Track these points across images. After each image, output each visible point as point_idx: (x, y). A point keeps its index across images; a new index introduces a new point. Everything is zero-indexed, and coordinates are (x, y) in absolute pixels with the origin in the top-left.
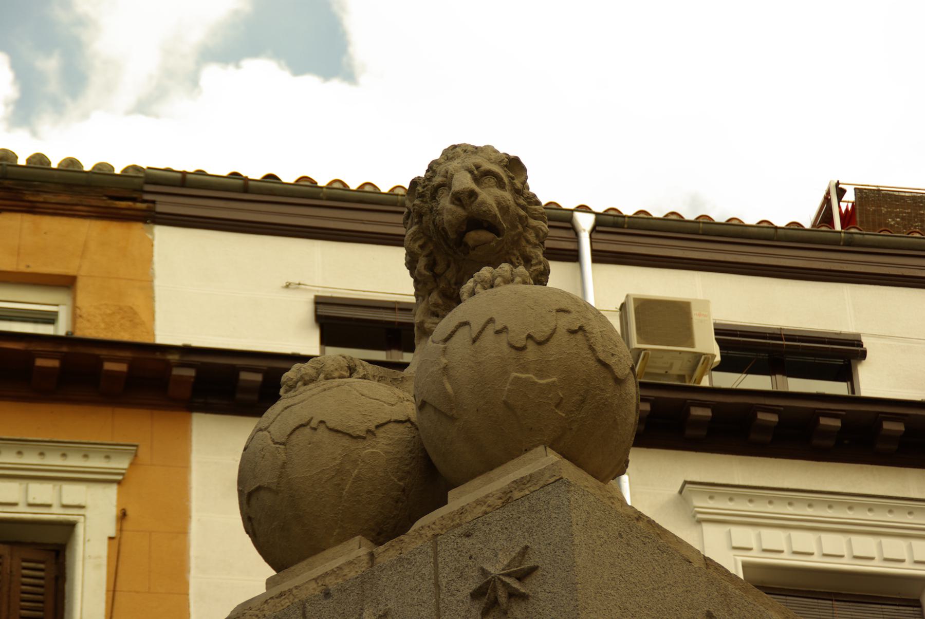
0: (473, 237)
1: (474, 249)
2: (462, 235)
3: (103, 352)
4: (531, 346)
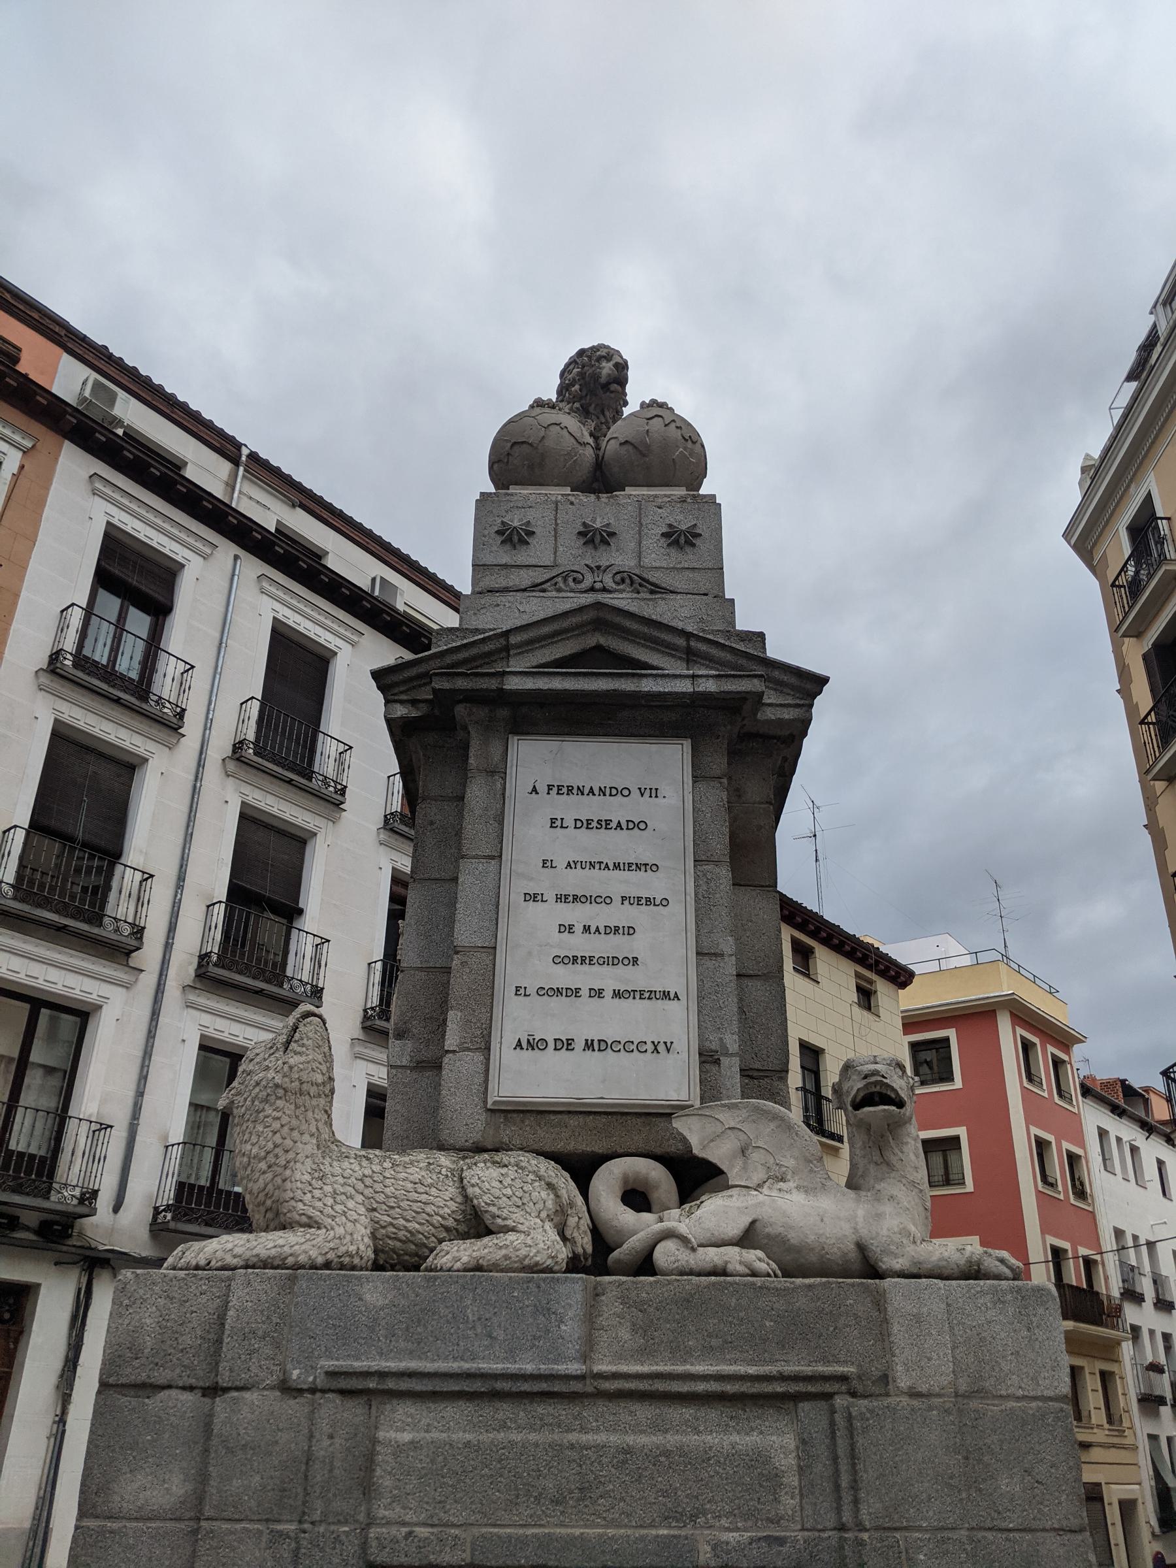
0: (614, 387)
1: (612, 392)
2: (608, 384)
3: (39, 391)
4: (689, 442)
